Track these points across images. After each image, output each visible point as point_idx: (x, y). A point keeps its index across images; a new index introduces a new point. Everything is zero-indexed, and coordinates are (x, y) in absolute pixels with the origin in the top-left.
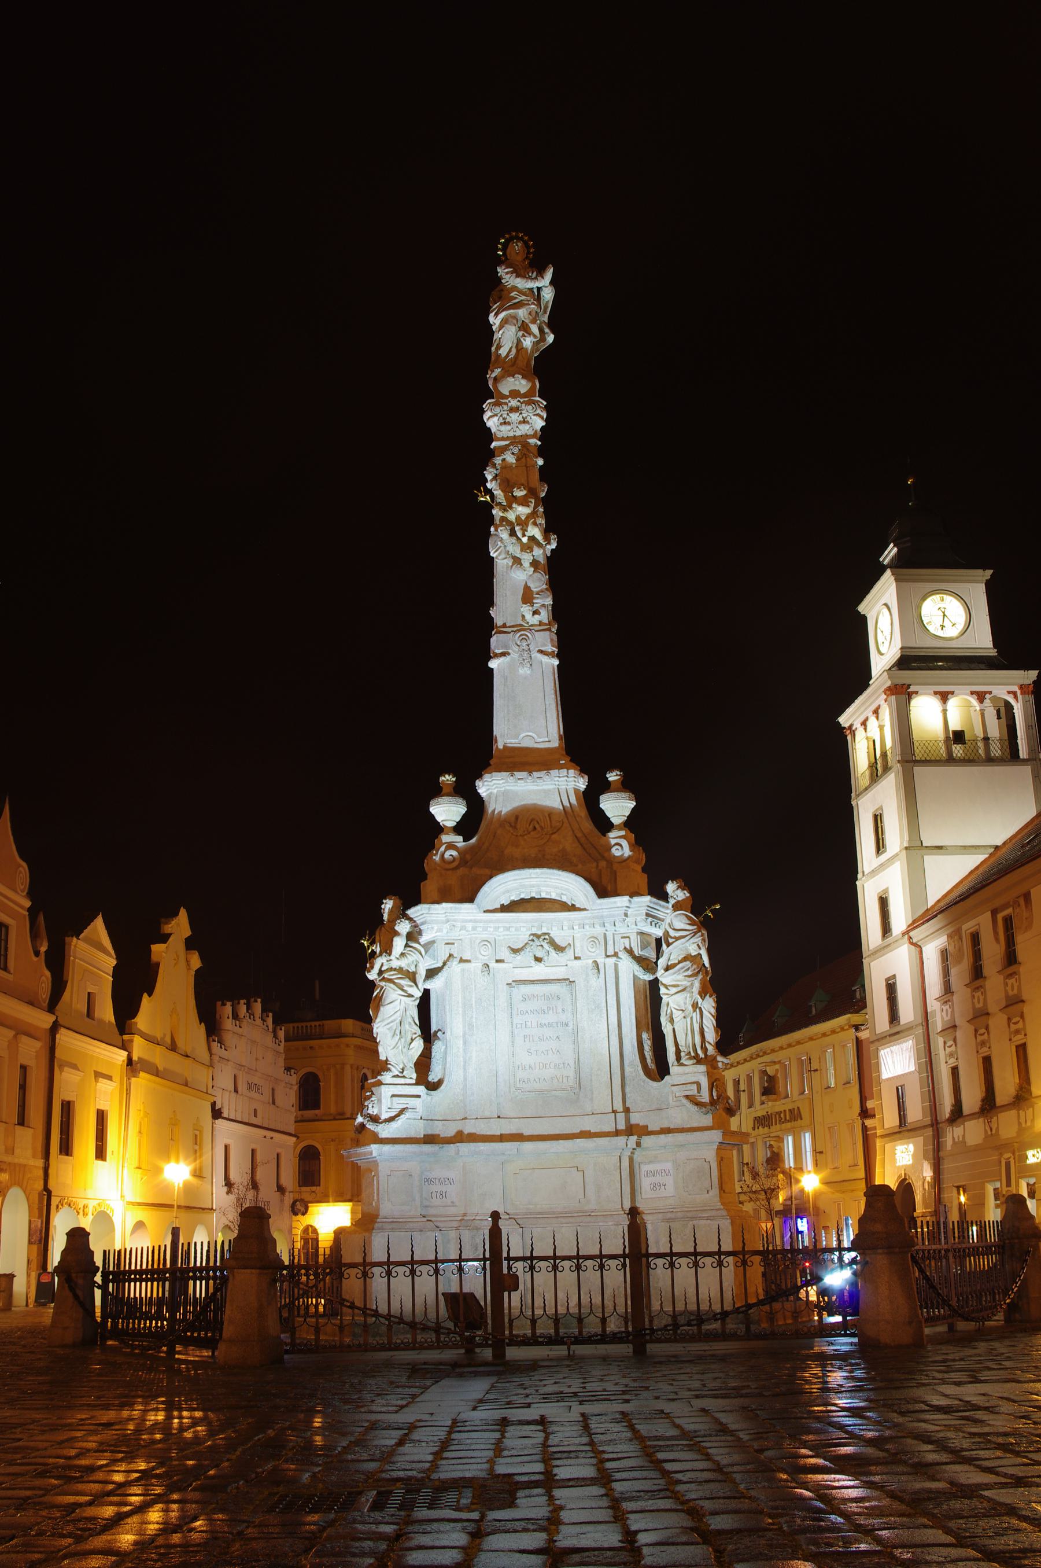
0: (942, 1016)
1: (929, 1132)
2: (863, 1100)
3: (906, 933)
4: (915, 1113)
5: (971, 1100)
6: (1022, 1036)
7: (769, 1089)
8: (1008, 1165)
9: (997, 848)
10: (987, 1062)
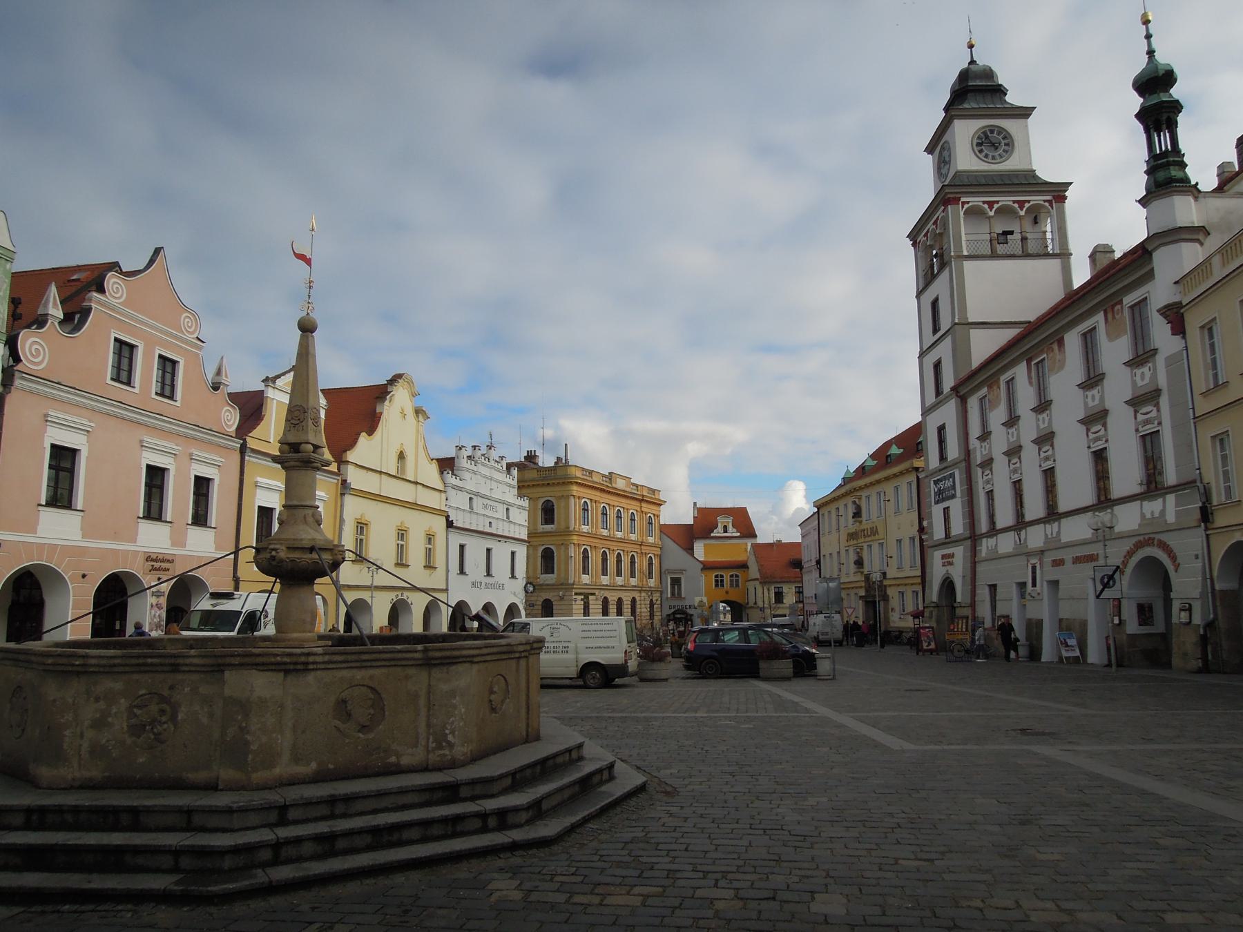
0: (981, 451)
1: (969, 543)
2: (920, 520)
3: (953, 389)
4: (958, 528)
5: (1005, 517)
6: (1052, 462)
7: (857, 514)
8: (1034, 568)
9: (1030, 322)
10: (1017, 486)
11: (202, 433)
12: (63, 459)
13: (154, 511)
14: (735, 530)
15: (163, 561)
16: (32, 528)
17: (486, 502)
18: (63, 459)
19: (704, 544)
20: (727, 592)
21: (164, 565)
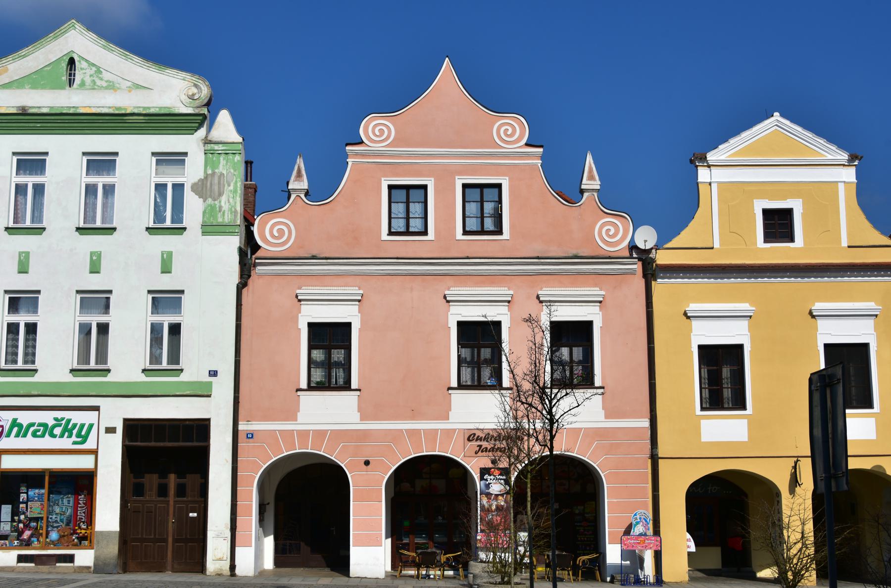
16: (291, 414)
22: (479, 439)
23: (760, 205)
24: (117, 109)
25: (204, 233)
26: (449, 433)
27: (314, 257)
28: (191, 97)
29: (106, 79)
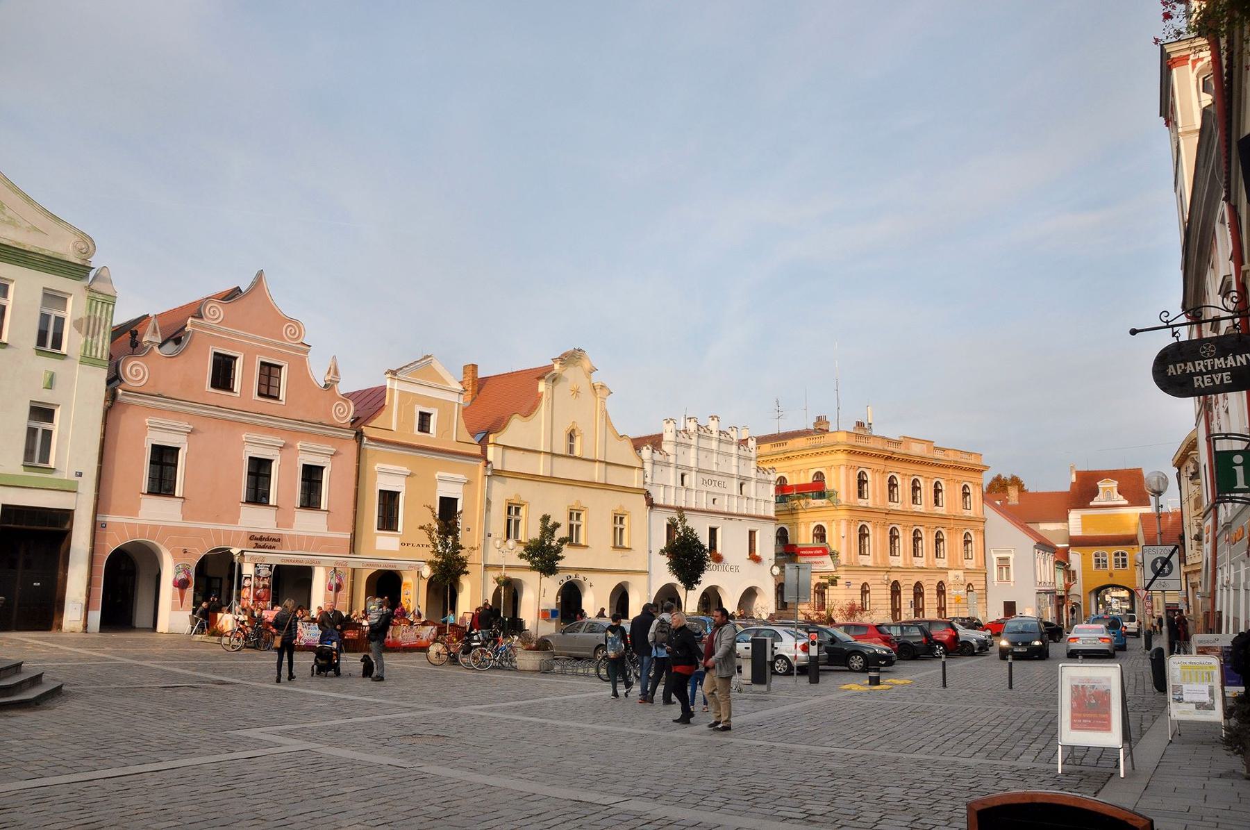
11: (323, 429)
12: (164, 458)
13: (258, 494)
14: (1121, 497)
15: (268, 539)
16: (134, 512)
17: (707, 477)
18: (164, 458)
19: (1082, 516)
20: (1111, 575)
21: (269, 543)
22: (256, 539)
23: (420, 408)
24: (17, 243)
25: (81, 362)
26: (238, 533)
27: (160, 396)
28: (80, 250)
29: (8, 215)
